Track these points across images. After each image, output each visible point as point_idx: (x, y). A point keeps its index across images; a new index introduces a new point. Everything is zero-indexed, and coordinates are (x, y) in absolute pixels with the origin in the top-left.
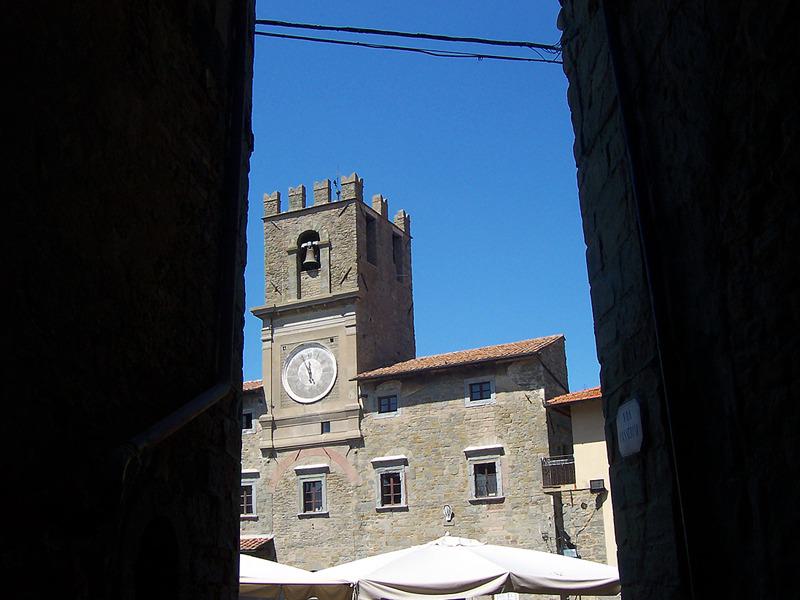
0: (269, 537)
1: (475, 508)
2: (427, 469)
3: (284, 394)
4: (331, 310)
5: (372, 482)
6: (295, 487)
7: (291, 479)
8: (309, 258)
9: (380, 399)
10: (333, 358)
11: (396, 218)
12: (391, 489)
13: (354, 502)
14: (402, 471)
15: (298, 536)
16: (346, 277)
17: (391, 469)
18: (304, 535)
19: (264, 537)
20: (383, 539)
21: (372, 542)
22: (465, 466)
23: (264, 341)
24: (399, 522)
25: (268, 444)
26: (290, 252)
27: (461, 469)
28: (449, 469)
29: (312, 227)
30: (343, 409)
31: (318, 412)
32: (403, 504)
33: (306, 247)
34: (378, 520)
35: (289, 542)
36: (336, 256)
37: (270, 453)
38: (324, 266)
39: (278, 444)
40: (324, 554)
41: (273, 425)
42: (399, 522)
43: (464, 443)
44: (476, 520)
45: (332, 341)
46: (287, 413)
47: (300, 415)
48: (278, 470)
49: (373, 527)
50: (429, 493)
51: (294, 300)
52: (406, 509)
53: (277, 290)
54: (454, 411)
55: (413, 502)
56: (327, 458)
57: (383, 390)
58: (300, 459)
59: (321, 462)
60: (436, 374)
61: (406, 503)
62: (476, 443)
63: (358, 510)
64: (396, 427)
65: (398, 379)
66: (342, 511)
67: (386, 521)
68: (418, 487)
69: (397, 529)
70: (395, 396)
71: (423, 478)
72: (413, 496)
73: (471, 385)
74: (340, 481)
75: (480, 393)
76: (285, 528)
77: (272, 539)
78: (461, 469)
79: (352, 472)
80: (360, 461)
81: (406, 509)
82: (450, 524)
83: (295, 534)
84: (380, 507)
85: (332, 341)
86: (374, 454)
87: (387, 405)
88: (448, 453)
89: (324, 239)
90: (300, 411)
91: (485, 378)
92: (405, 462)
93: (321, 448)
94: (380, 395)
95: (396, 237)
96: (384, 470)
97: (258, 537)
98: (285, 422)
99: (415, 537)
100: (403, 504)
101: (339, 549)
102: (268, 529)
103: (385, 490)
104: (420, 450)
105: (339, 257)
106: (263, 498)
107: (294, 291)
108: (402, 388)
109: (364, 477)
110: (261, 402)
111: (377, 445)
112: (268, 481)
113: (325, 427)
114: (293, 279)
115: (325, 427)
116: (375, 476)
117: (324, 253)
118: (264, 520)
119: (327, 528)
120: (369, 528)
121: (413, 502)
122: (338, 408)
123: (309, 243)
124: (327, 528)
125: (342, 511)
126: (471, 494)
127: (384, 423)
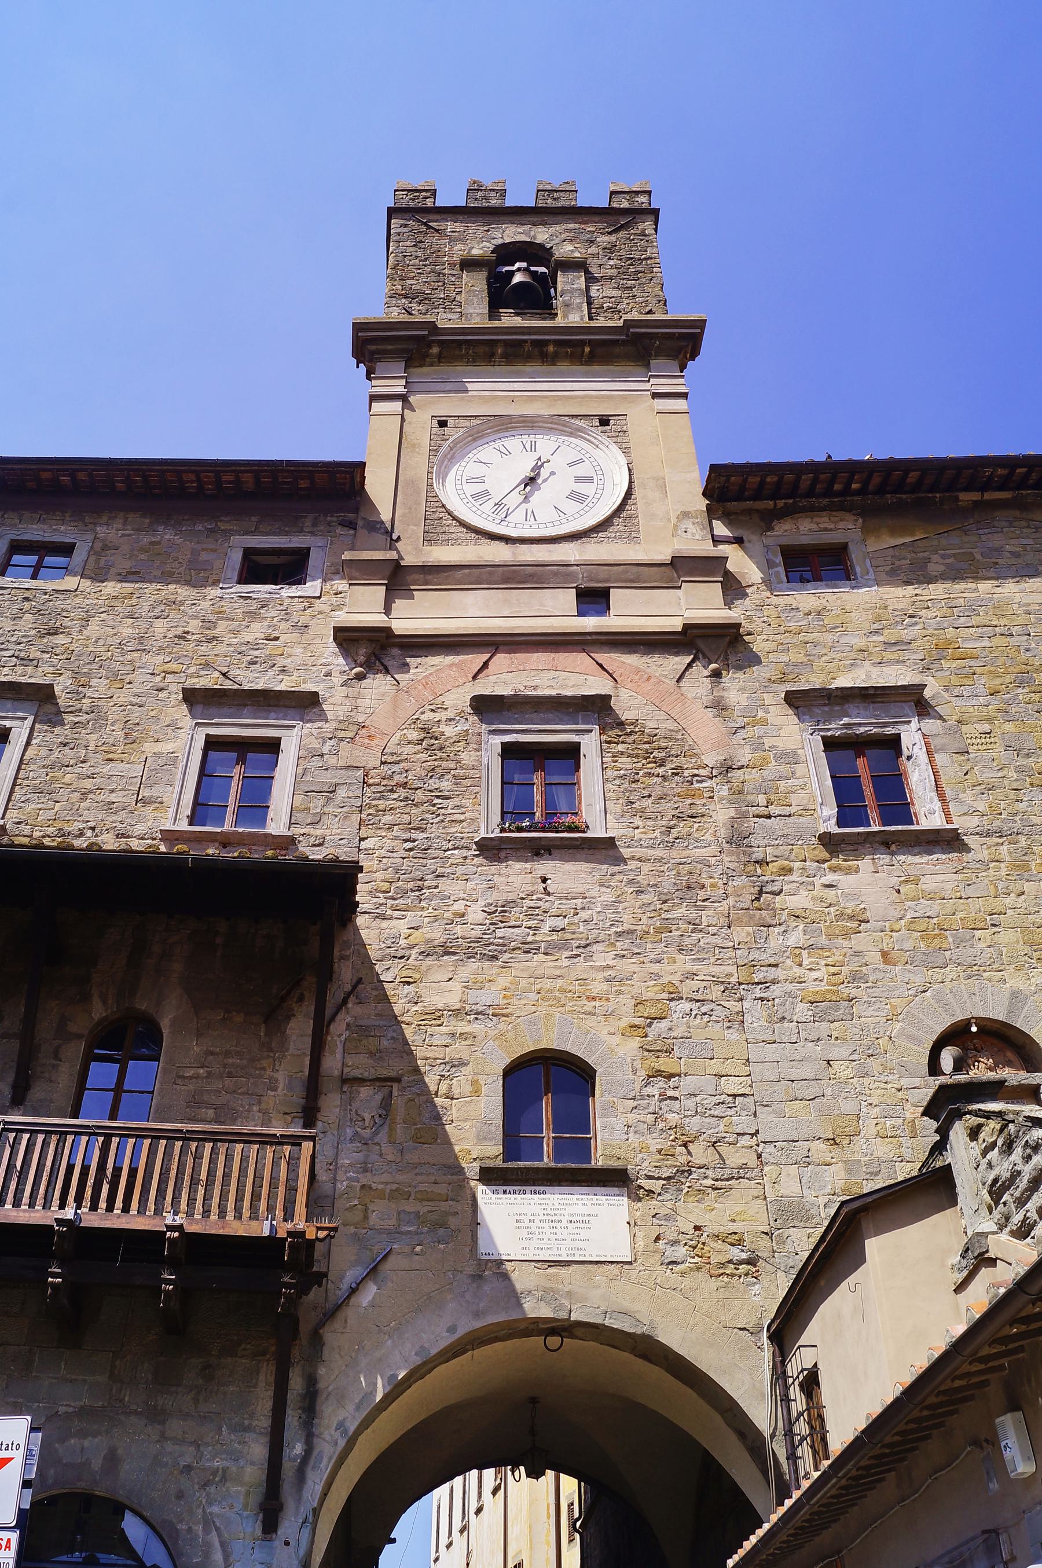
2: (1009, 727)
5: (790, 758)
6: (468, 757)
7: (450, 731)
12: (871, 795)
13: (721, 814)
14: (911, 735)
15: (476, 914)
17: (863, 723)
18: (499, 914)
20: (865, 942)
23: (374, 398)
24: (928, 884)
35: (437, 935)
40: (598, 988)
41: (399, 580)
42: (928, 884)
48: (395, 703)
52: (947, 841)
60: (976, 504)
65: (849, 510)
66: (670, 838)
68: (981, 774)
69: (925, 907)
74: (656, 754)
81: (947, 841)
83: (459, 906)
87: (814, 565)
90: (500, 553)
94: (785, 541)
96: (835, 728)
98: (437, 575)
103: (845, 789)
106: (328, 778)
108: (866, 531)
109: (757, 745)
110: (352, 525)
113: (593, 598)
115: (593, 598)
119: (608, 895)
124: (608, 895)
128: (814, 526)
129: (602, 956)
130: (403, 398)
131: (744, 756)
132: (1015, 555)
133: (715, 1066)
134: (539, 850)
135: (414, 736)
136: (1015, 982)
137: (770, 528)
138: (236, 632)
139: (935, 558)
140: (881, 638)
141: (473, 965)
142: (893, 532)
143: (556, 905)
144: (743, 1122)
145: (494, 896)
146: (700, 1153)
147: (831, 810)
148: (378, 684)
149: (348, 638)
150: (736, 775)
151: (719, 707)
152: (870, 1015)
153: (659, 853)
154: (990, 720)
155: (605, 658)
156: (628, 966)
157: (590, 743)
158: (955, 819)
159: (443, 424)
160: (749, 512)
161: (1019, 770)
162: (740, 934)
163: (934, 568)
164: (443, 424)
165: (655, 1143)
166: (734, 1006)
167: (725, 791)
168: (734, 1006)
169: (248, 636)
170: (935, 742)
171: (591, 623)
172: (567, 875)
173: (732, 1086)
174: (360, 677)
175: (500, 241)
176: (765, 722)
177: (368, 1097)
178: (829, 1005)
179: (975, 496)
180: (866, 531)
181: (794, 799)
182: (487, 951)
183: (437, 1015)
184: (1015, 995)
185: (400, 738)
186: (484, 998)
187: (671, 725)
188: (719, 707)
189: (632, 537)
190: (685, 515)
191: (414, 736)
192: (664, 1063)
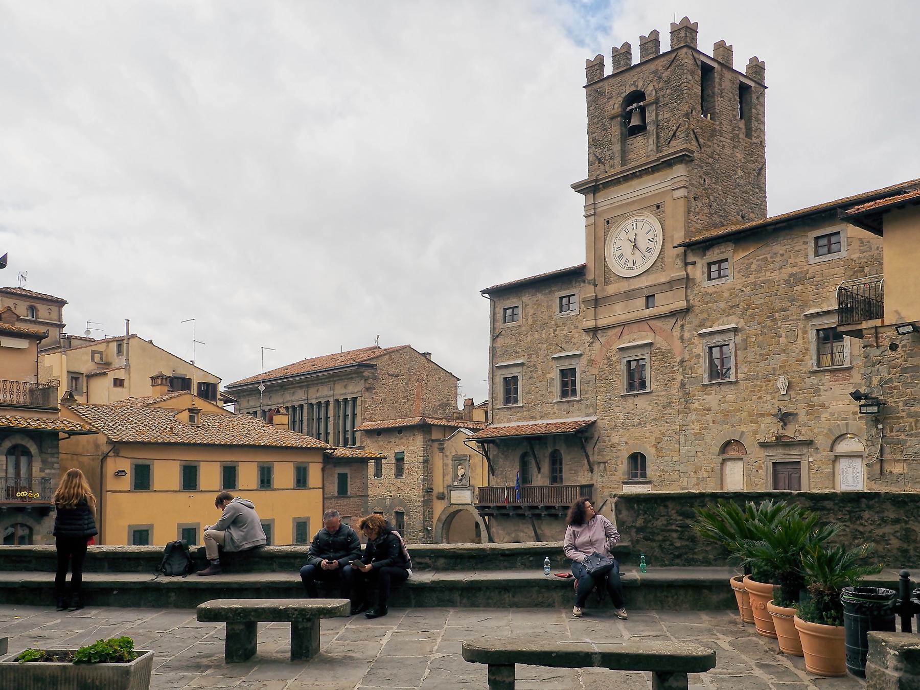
0: (593, 419)
1: (814, 380)
2: (761, 338)
3: (607, 272)
4: (656, 175)
5: (698, 356)
7: (614, 359)
8: (635, 121)
9: (710, 265)
10: (657, 226)
11: (740, 64)
13: (680, 378)
15: (621, 417)
16: (674, 135)
19: (587, 419)
21: (698, 421)
22: (805, 332)
25: (591, 324)
26: (613, 118)
27: (800, 335)
28: (787, 337)
29: (637, 86)
30: (668, 279)
31: (642, 285)
32: (732, 378)
33: (631, 110)
34: (705, 397)
36: (665, 115)
37: (594, 331)
38: (651, 128)
39: (602, 323)
40: (648, 435)
43: (805, 305)
44: (817, 391)
45: (658, 207)
46: (611, 289)
47: (623, 290)
49: (700, 405)
50: (762, 364)
51: (619, 168)
53: (600, 161)
54: (795, 270)
55: (743, 375)
56: (651, 334)
57: (714, 254)
58: (624, 337)
59: (645, 338)
61: (736, 377)
62: (819, 306)
63: (683, 385)
64: (726, 295)
66: (667, 387)
67: (712, 399)
69: (725, 406)
70: (726, 260)
71: (755, 348)
72: (744, 368)
73: (817, 239)
75: (826, 245)
76: (608, 408)
77: (594, 422)
78: (800, 335)
79: (677, 346)
80: (687, 335)
81: (736, 383)
82: (786, 398)
84: (706, 382)
85: (658, 207)
86: (702, 325)
87: (716, 269)
88: (785, 319)
89: (649, 99)
90: (624, 287)
91: (834, 229)
92: (735, 330)
93: (644, 326)
95: (744, 90)
97: (581, 419)
99: (745, 414)
100: (732, 378)
101: (663, 429)
102: (592, 410)
104: (753, 317)
105: (667, 116)
107: (617, 160)
109: (690, 351)
111: (706, 316)
112: (591, 362)
113: (649, 299)
114: (617, 148)
115: (649, 299)
116: (700, 348)
117: (650, 116)
118: (588, 402)
120: (695, 405)
121: (743, 375)
122: (663, 279)
123: (635, 105)
125: (667, 387)
126: (811, 362)
127: (711, 290)
128: (718, 251)
129: (649, 427)
130: (594, 214)
131: (687, 357)
132: (782, 255)
133: (672, 454)
134: (635, 396)
135: (606, 362)
136: (744, 430)
137: (705, 255)
138: (561, 331)
139: (755, 262)
140: (730, 304)
141: (621, 431)
142: (743, 251)
143: (639, 412)
144: (677, 468)
145: (626, 411)
146: (666, 476)
147: (706, 376)
148: (597, 345)
149: (587, 331)
150: (684, 364)
151: (682, 338)
152: (708, 438)
153: (663, 393)
154: (755, 335)
155: (652, 323)
156: (654, 428)
157: (647, 357)
158: (739, 376)
159: (608, 222)
160: (699, 248)
161: (760, 355)
162: (681, 416)
163: (753, 267)
164: (608, 222)
165: (658, 474)
166: (677, 437)
167: (681, 370)
168: (677, 437)
169: (565, 332)
170: (738, 346)
171: (647, 312)
172: (642, 403)
173: (675, 459)
174: (592, 343)
175: (624, 95)
176: (693, 343)
177: (602, 465)
178: (699, 436)
179: (773, 227)
180: (735, 251)
181: (698, 371)
182: (623, 427)
183: (613, 445)
184: (743, 432)
185: (602, 363)
186: (623, 440)
187: (669, 348)
188: (682, 338)
189: (663, 269)
190: (678, 255)
191: (606, 362)
192: (661, 454)
